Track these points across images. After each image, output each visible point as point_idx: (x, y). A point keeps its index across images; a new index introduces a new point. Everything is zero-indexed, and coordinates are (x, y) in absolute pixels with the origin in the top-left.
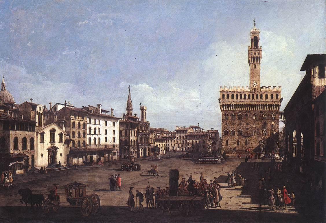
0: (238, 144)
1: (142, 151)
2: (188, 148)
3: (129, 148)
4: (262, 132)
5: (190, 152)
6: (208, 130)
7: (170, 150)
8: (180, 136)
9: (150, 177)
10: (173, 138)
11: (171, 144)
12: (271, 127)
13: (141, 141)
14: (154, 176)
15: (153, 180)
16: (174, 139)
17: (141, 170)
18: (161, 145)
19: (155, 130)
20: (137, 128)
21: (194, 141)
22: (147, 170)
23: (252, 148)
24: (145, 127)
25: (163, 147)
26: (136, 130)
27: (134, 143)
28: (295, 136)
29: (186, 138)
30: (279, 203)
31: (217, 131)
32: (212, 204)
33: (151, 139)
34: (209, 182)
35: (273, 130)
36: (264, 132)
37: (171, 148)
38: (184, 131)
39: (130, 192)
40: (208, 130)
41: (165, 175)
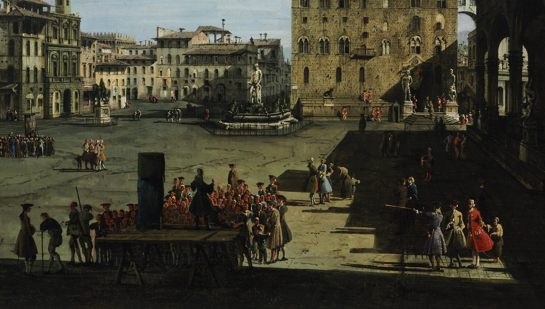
0: (339, 79)
1: (57, 98)
2: (192, 91)
3: (19, 88)
4: (409, 43)
5: (198, 101)
6: (252, 39)
7: (138, 98)
8: (169, 55)
9: (80, 174)
10: (148, 59)
11: (144, 79)
12: (435, 31)
13: (55, 69)
14: (92, 170)
15: (88, 181)
16: (153, 63)
17: (56, 153)
18: (115, 81)
19: (95, 39)
20: (43, 31)
21: (211, 70)
22: (72, 153)
23: (377, 90)
24: (66, 30)
25: (121, 87)
26: (42, 37)
27: (36, 76)
28: (505, 56)
29: (186, 62)
30: (456, 251)
31: (279, 41)
32: (263, 253)
33: (84, 65)
34: (254, 190)
35: (441, 38)
36: (415, 44)
37: (142, 91)
38: (182, 43)
39: (24, 219)
40: (252, 39)
41: (125, 168)
